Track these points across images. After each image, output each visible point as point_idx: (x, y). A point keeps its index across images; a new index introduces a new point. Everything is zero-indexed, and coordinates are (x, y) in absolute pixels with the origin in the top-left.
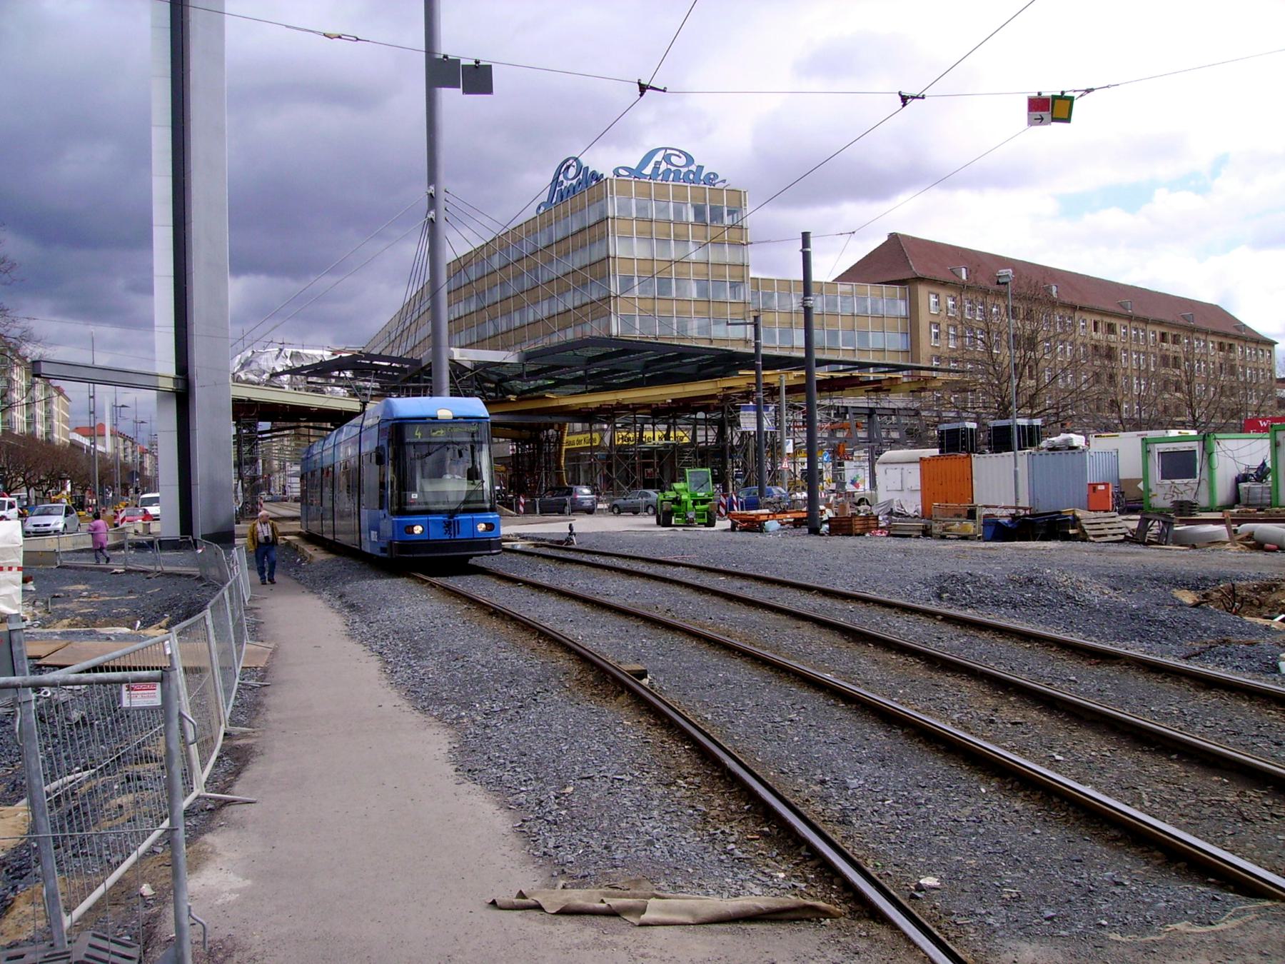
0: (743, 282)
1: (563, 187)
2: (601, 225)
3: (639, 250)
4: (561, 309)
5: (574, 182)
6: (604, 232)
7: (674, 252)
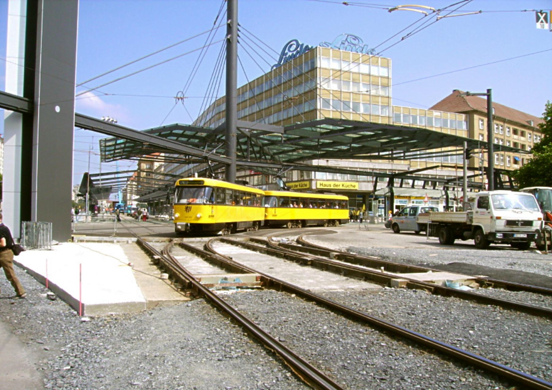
0: (388, 106)
1: (287, 56)
2: (312, 72)
3: (334, 86)
4: (285, 117)
5: (295, 53)
6: (314, 76)
7: (352, 88)
